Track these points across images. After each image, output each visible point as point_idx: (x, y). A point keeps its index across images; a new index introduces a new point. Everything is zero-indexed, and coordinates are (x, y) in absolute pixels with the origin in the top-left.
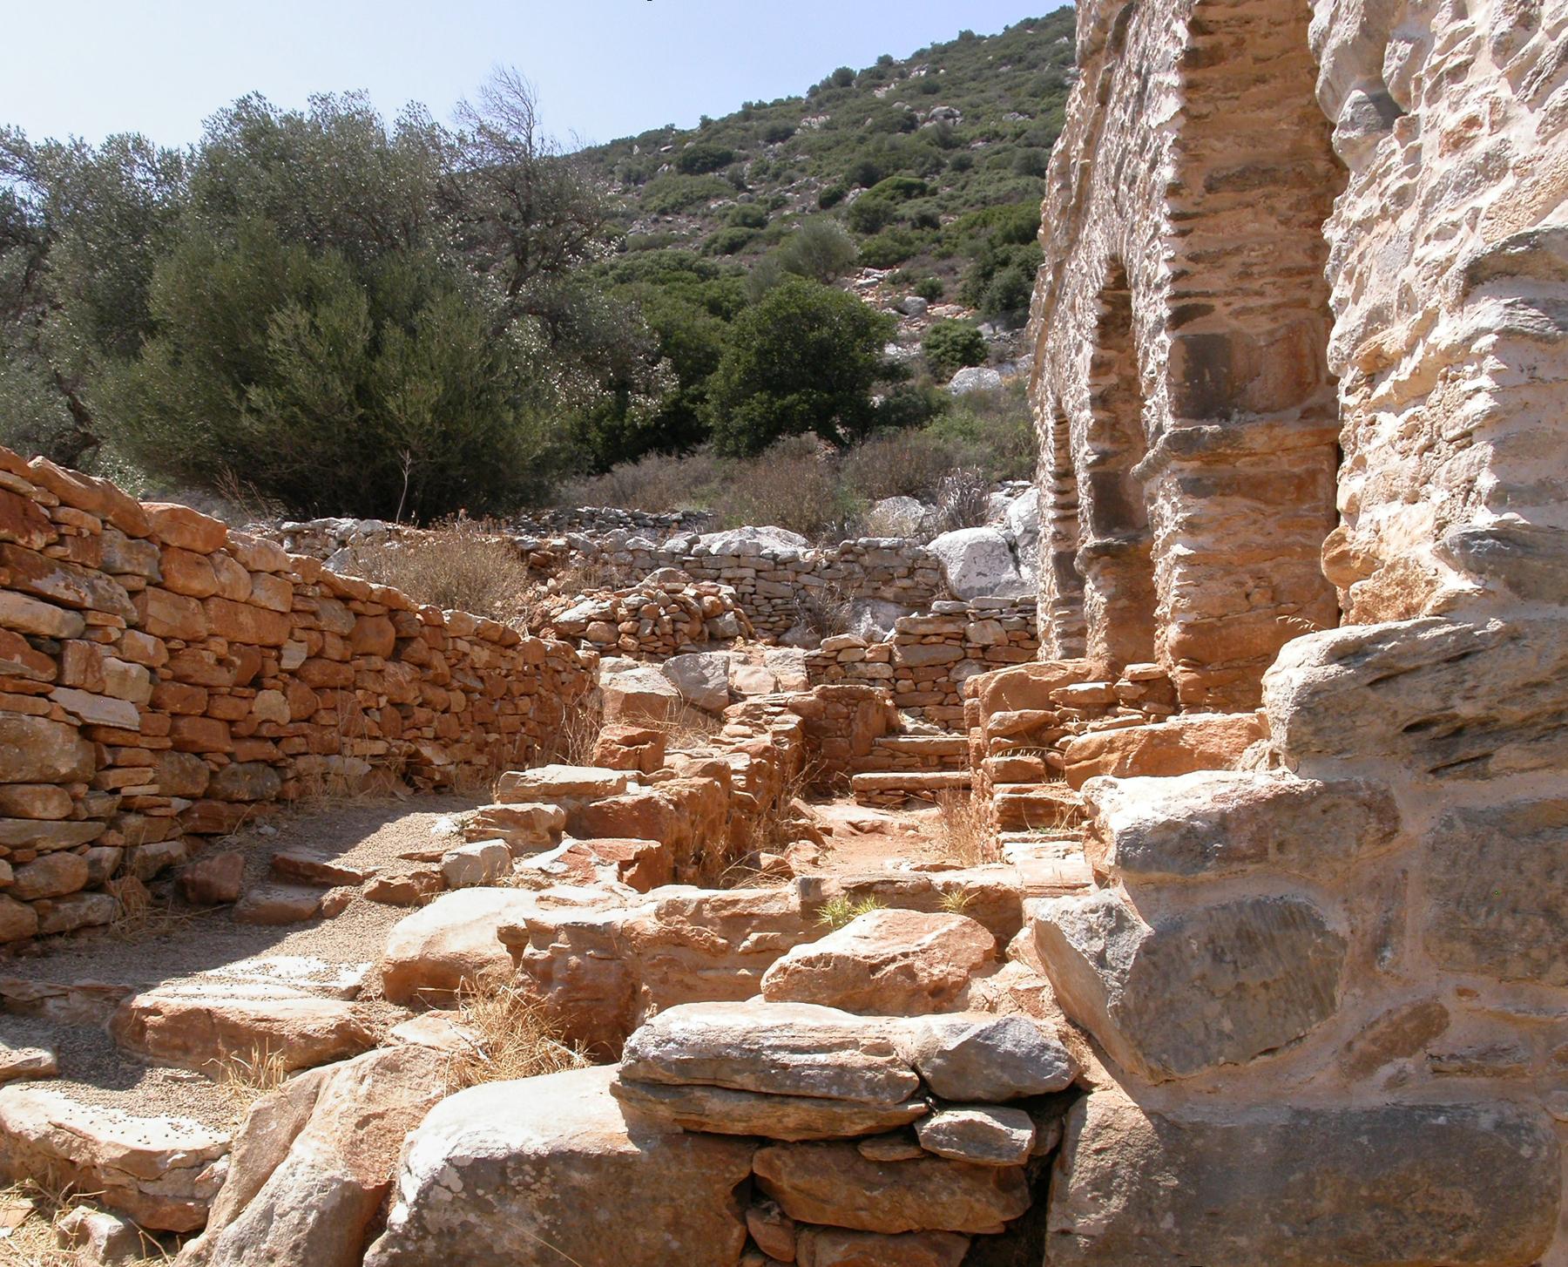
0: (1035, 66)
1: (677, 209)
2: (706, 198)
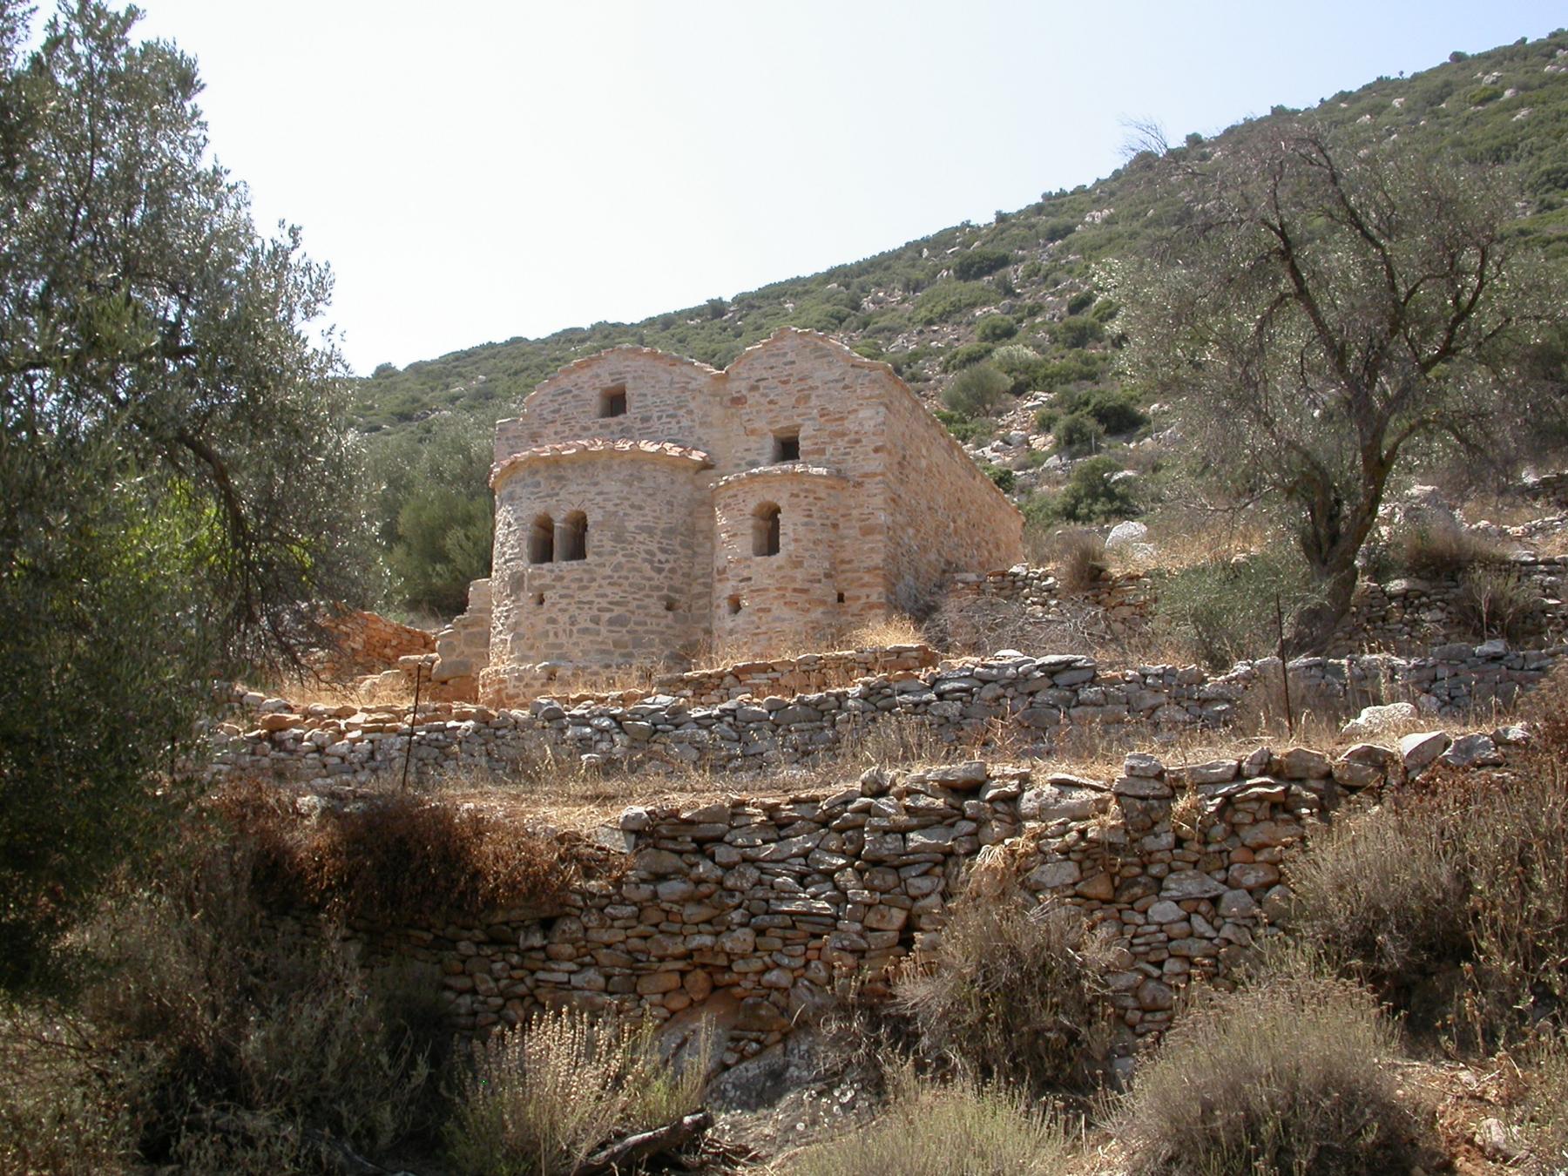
1: (944, 317)
2: (973, 305)
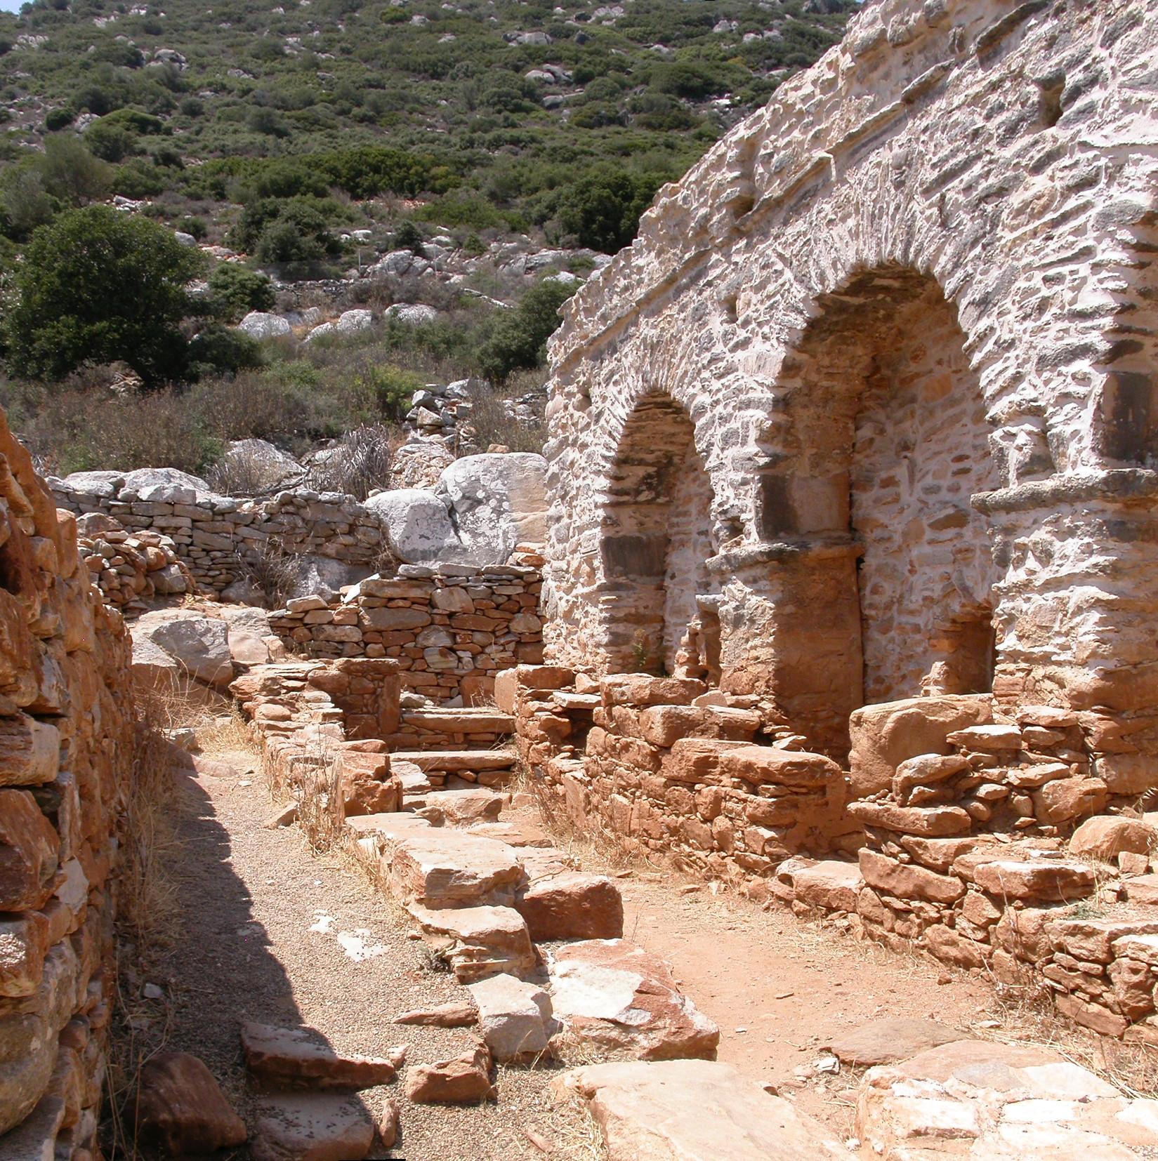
0: (254, 29)
